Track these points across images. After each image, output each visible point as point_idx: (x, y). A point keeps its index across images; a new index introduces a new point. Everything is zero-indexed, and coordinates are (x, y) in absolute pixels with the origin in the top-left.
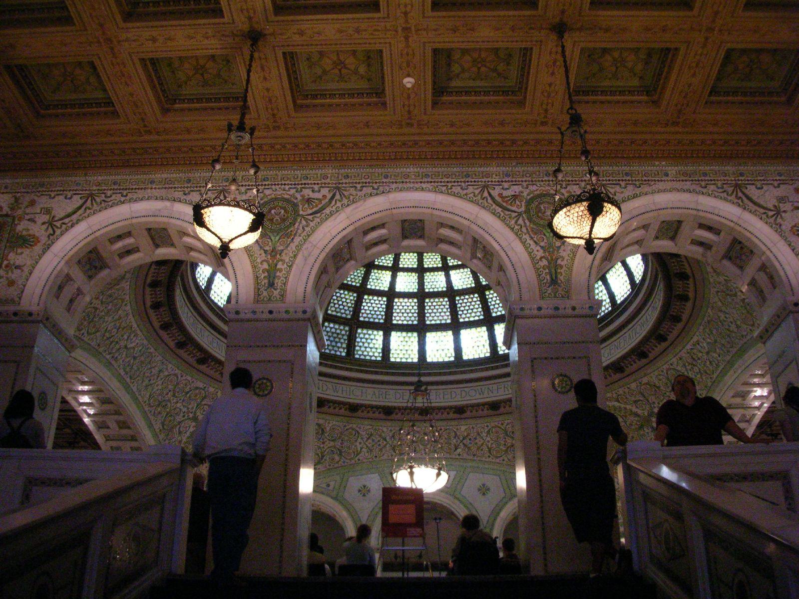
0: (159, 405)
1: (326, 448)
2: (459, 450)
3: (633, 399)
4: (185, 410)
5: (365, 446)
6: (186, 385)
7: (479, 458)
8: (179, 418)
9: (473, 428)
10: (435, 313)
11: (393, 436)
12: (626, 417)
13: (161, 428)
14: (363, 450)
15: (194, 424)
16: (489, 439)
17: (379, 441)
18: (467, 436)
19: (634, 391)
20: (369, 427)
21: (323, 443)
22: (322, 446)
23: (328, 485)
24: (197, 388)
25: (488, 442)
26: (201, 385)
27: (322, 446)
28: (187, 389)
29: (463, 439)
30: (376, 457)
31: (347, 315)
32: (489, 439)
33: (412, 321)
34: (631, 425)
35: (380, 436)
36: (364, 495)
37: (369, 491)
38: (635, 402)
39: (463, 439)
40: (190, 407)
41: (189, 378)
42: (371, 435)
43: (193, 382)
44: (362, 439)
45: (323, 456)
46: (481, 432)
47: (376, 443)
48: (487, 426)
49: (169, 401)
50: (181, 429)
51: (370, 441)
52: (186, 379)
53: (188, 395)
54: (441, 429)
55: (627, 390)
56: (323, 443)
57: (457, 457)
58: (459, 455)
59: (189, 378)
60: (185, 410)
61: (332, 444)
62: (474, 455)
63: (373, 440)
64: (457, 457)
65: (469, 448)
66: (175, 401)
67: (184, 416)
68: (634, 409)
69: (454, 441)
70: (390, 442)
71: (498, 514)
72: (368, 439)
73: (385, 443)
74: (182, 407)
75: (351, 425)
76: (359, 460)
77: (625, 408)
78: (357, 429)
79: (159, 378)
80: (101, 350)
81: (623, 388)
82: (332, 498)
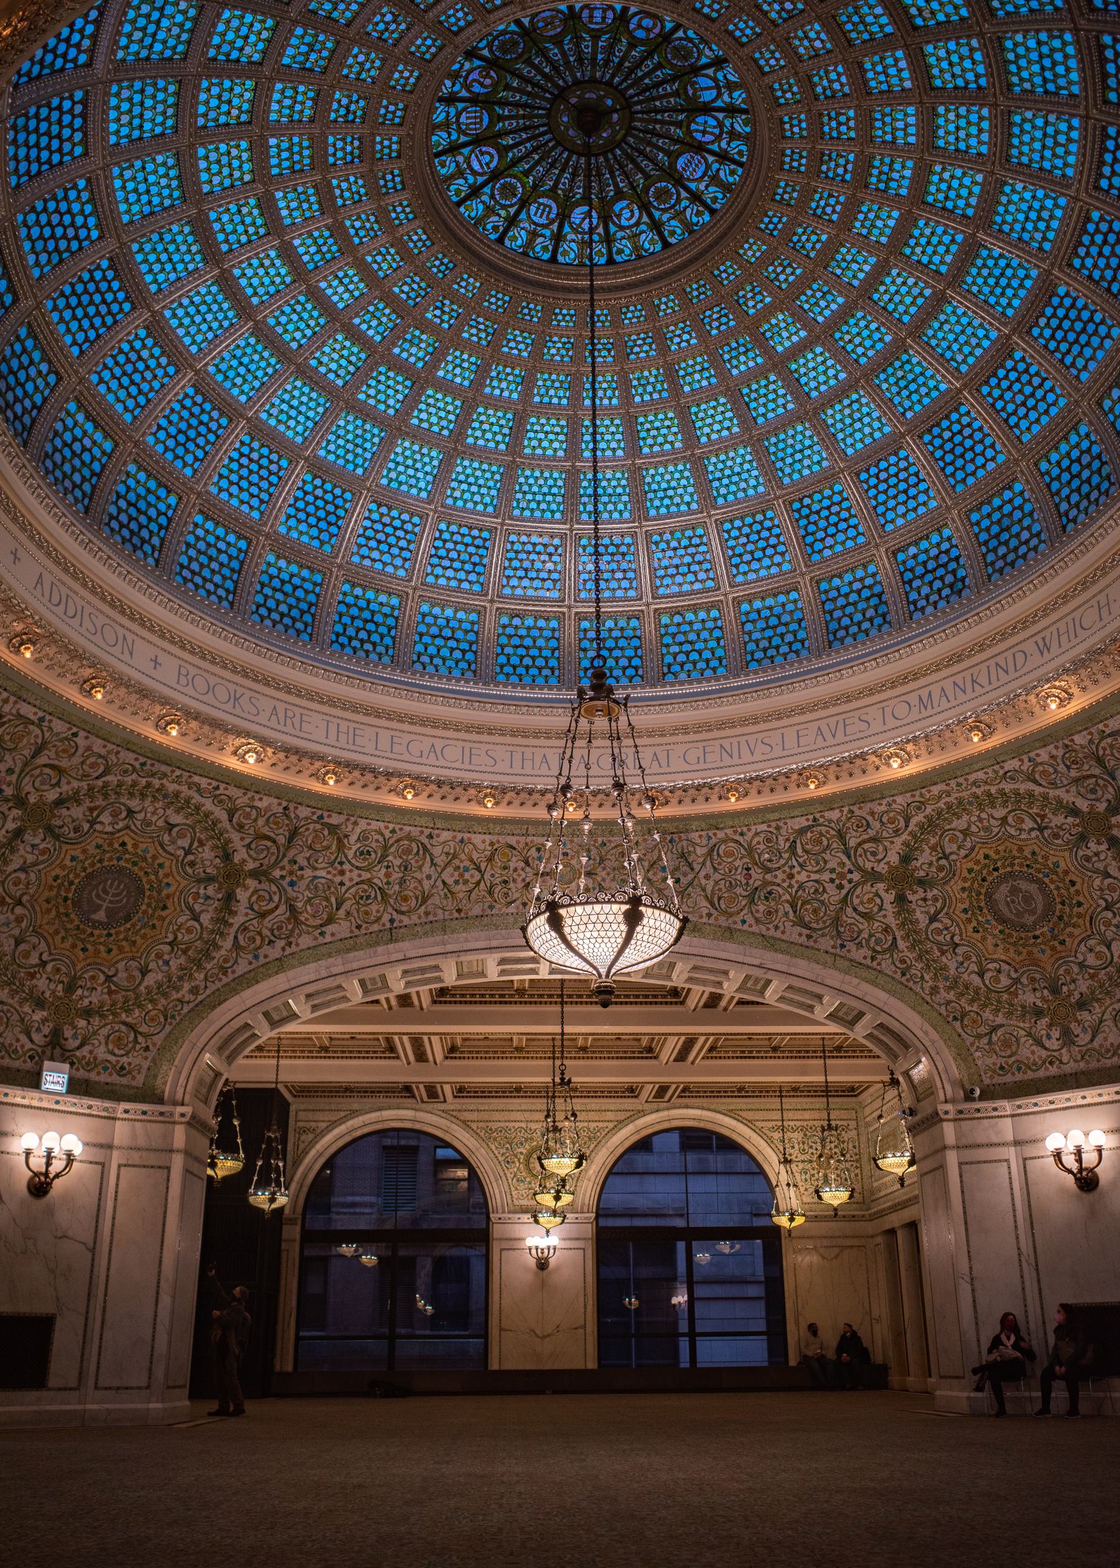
0: (752, 902)
4: (826, 876)
6: (769, 840)
8: (833, 895)
13: (806, 932)
15: (881, 887)
24: (802, 831)
26: (802, 822)
28: (783, 845)
40: (830, 865)
41: (764, 827)
43: (778, 828)
49: (766, 883)
50: (861, 909)
52: (757, 834)
53: (799, 851)
59: (764, 827)
60: (826, 876)
66: (781, 875)
67: (840, 887)
74: (814, 877)
79: (697, 867)
80: (477, 910)
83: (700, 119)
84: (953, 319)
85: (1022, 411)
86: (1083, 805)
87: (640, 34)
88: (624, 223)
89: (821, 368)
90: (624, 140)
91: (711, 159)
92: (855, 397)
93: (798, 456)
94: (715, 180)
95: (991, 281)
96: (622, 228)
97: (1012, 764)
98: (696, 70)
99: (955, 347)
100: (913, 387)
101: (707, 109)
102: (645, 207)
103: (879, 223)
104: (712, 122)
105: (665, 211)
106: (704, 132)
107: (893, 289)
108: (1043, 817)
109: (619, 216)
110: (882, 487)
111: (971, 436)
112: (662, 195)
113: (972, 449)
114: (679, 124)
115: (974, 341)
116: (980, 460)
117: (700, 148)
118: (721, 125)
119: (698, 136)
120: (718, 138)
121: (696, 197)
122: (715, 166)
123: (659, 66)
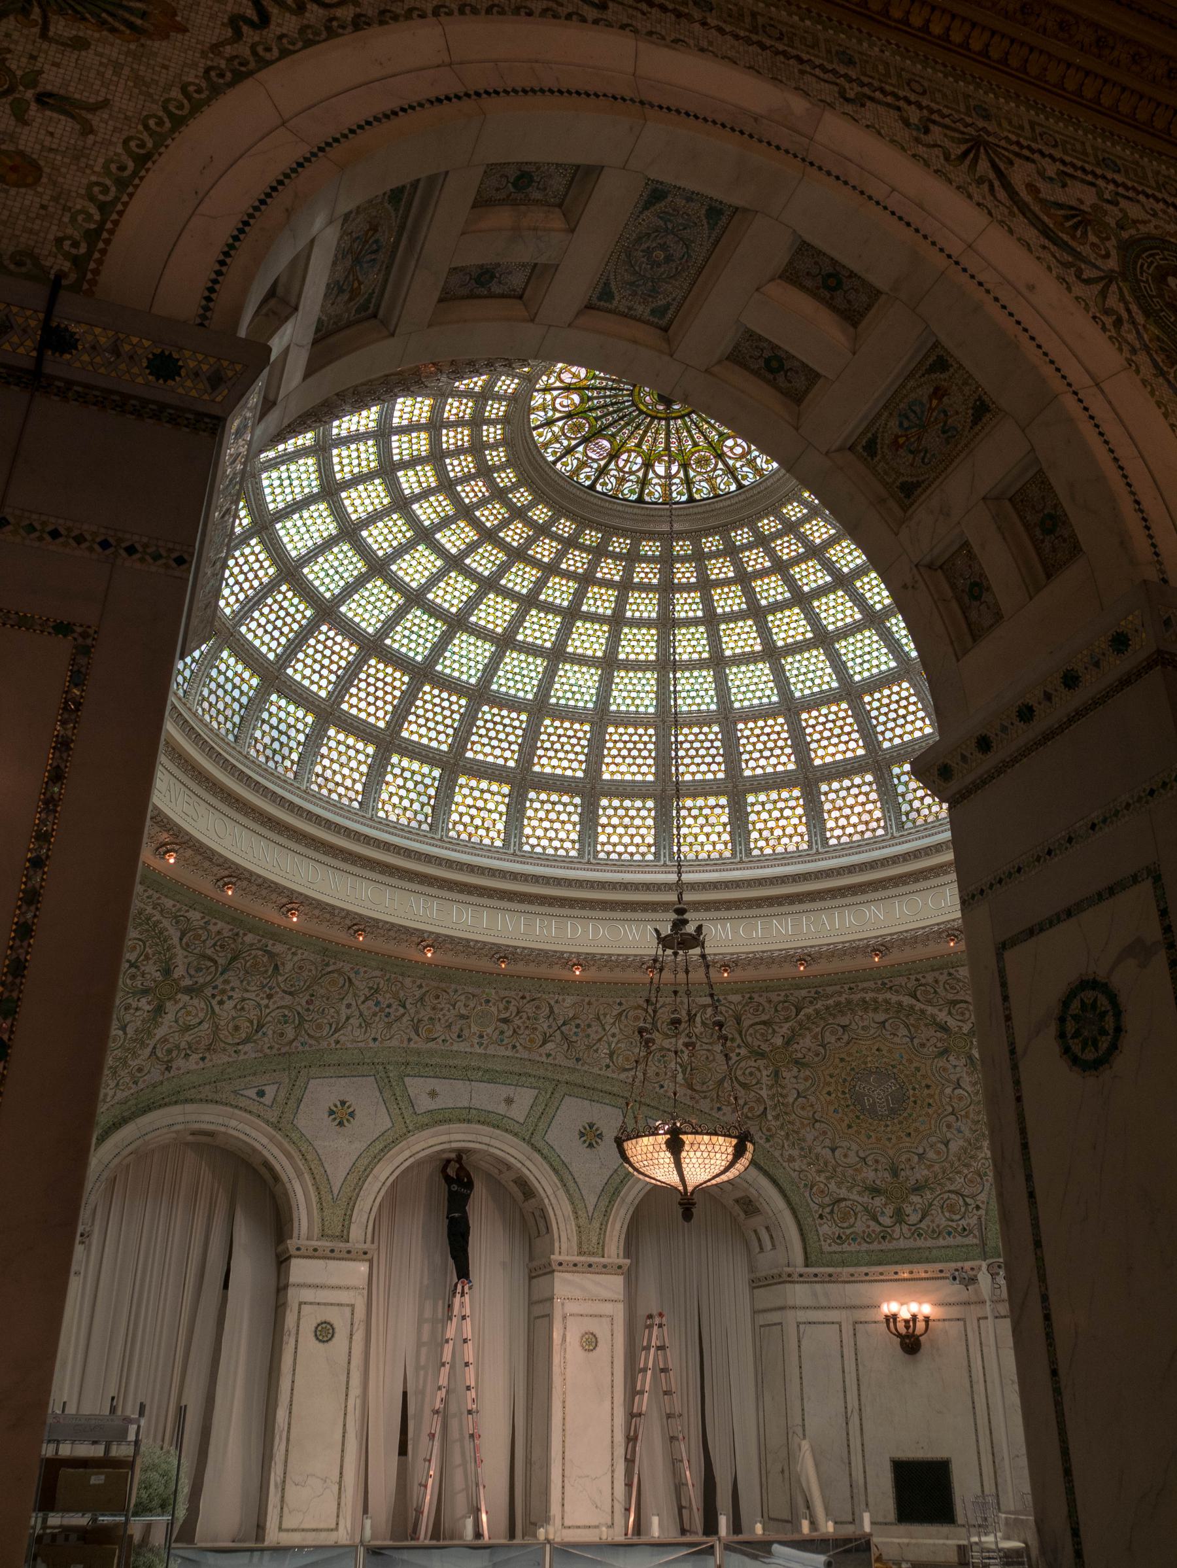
1: (272, 1007)
2: (550, 1046)
3: (950, 997)
5: (357, 1013)
7: (586, 1067)
9: (589, 1003)
10: (556, 751)
11: (422, 999)
12: (917, 1028)
14: (351, 1021)
16: (617, 1031)
17: (389, 1006)
18: (574, 1018)
19: (959, 980)
20: (378, 973)
21: (269, 997)
22: (265, 1002)
23: (261, 1094)
25: (614, 1035)
27: (265, 1002)
29: (564, 1024)
30: (375, 1039)
31: (378, 719)
32: (617, 1031)
33: (506, 760)
34: (923, 1045)
35: (395, 996)
36: (341, 1124)
37: (352, 1114)
38: (954, 1003)
39: (564, 1024)
42: (376, 991)
44: (355, 995)
45: (260, 1026)
46: (605, 1015)
47: (382, 1010)
48: (620, 1004)
51: (370, 1003)
54: (523, 997)
55: (943, 978)
56: (269, 997)
57: (544, 1059)
58: (548, 1055)
61: (288, 1000)
62: (578, 1060)
63: (377, 1003)
64: (544, 1059)
65: (570, 1043)
68: (942, 1016)
69: (545, 1026)
70: (412, 1011)
71: (617, 1191)
72: (367, 999)
73: (402, 1010)
75: (340, 964)
76: (337, 1042)
77: (923, 1011)
78: (352, 975)
81: (936, 974)
82: (267, 1122)
83: (639, 460)
84: (479, 651)
85: (422, 721)
86: (179, 972)
87: (730, 443)
88: (558, 401)
89: (420, 568)
90: (638, 409)
91: (602, 463)
92: (396, 598)
93: (331, 572)
94: (583, 464)
95: (517, 670)
96: (554, 399)
97: (190, 914)
98: (685, 466)
99: (456, 657)
100: (414, 637)
101: (648, 465)
102: (569, 416)
103: (557, 594)
104: (635, 468)
105: (562, 429)
106: (627, 461)
107: (499, 606)
108: (147, 958)
109: (567, 397)
110: (320, 647)
111: (386, 693)
112: (577, 428)
113: (377, 698)
114: (639, 445)
115: (464, 669)
116: (372, 709)
117: (613, 456)
118: (631, 473)
119: (625, 456)
120: (620, 470)
121: (569, 451)
122: (595, 465)
123: (695, 444)
